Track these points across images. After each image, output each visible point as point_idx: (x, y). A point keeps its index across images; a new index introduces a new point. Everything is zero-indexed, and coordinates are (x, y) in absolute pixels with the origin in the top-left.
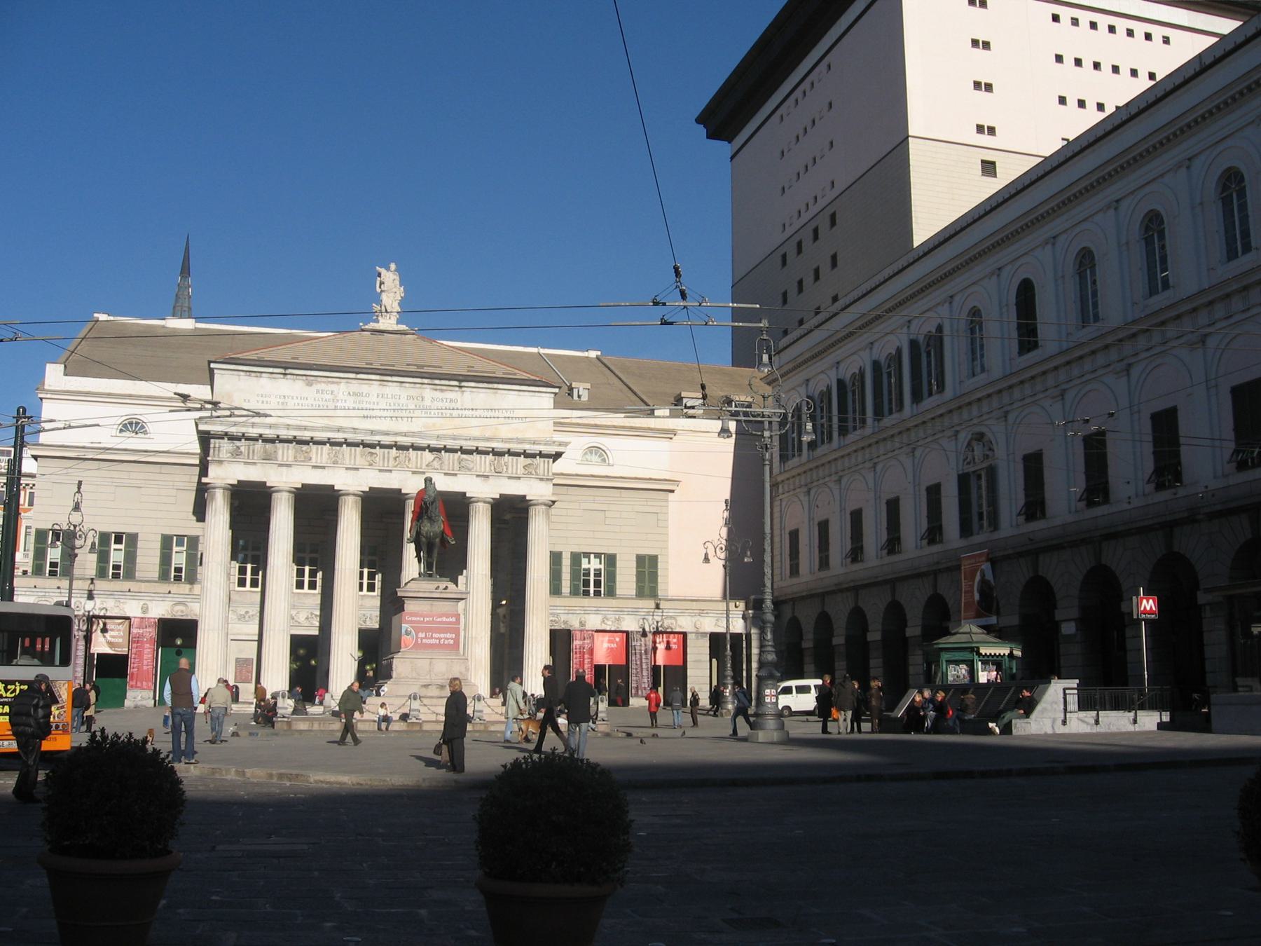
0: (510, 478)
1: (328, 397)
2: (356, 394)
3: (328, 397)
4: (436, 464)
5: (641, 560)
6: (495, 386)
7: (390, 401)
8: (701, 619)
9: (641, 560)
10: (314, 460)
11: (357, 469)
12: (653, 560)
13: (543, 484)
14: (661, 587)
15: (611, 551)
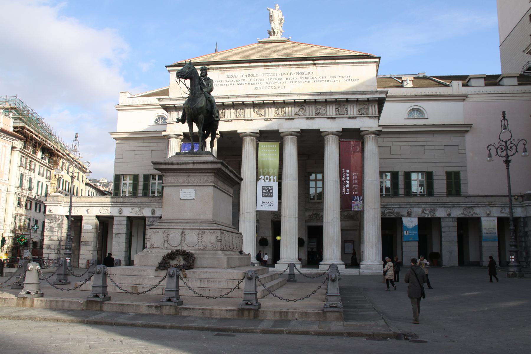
0: (349, 118)
1: (233, 79)
2: (250, 76)
3: (233, 79)
4: (301, 113)
5: (449, 174)
6: (337, 61)
7: (270, 77)
8: (491, 209)
9: (449, 174)
10: (226, 117)
11: (251, 120)
12: (457, 174)
13: (372, 120)
14: (463, 191)
15: (430, 170)
